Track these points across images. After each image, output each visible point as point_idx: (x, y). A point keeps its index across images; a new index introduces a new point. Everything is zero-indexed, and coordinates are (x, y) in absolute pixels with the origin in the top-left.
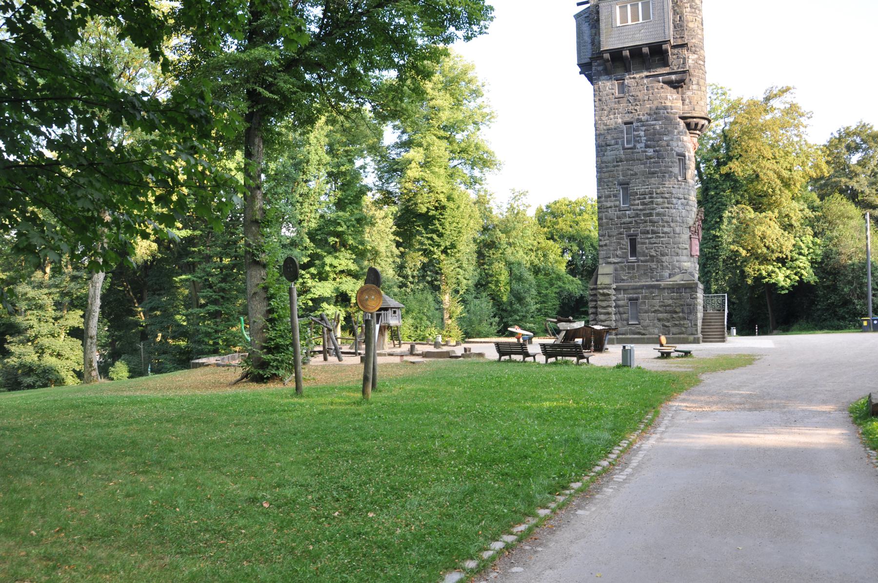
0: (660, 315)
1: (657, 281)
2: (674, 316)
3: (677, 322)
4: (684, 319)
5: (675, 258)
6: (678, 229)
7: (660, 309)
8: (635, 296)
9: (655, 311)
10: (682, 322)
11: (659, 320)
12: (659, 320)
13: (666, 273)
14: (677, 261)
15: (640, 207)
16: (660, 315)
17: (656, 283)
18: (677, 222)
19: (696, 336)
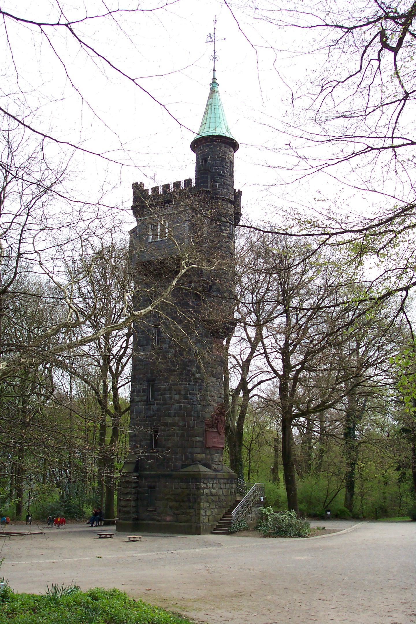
0: (171, 504)
1: (172, 471)
2: (182, 504)
3: (184, 511)
4: (190, 507)
5: (188, 450)
6: (192, 423)
7: (172, 497)
8: (154, 484)
9: (168, 499)
10: (188, 511)
11: (171, 508)
12: (171, 508)
13: (179, 464)
14: (190, 453)
15: (161, 402)
16: (171, 504)
17: (171, 473)
18: (191, 416)
19: (198, 525)
